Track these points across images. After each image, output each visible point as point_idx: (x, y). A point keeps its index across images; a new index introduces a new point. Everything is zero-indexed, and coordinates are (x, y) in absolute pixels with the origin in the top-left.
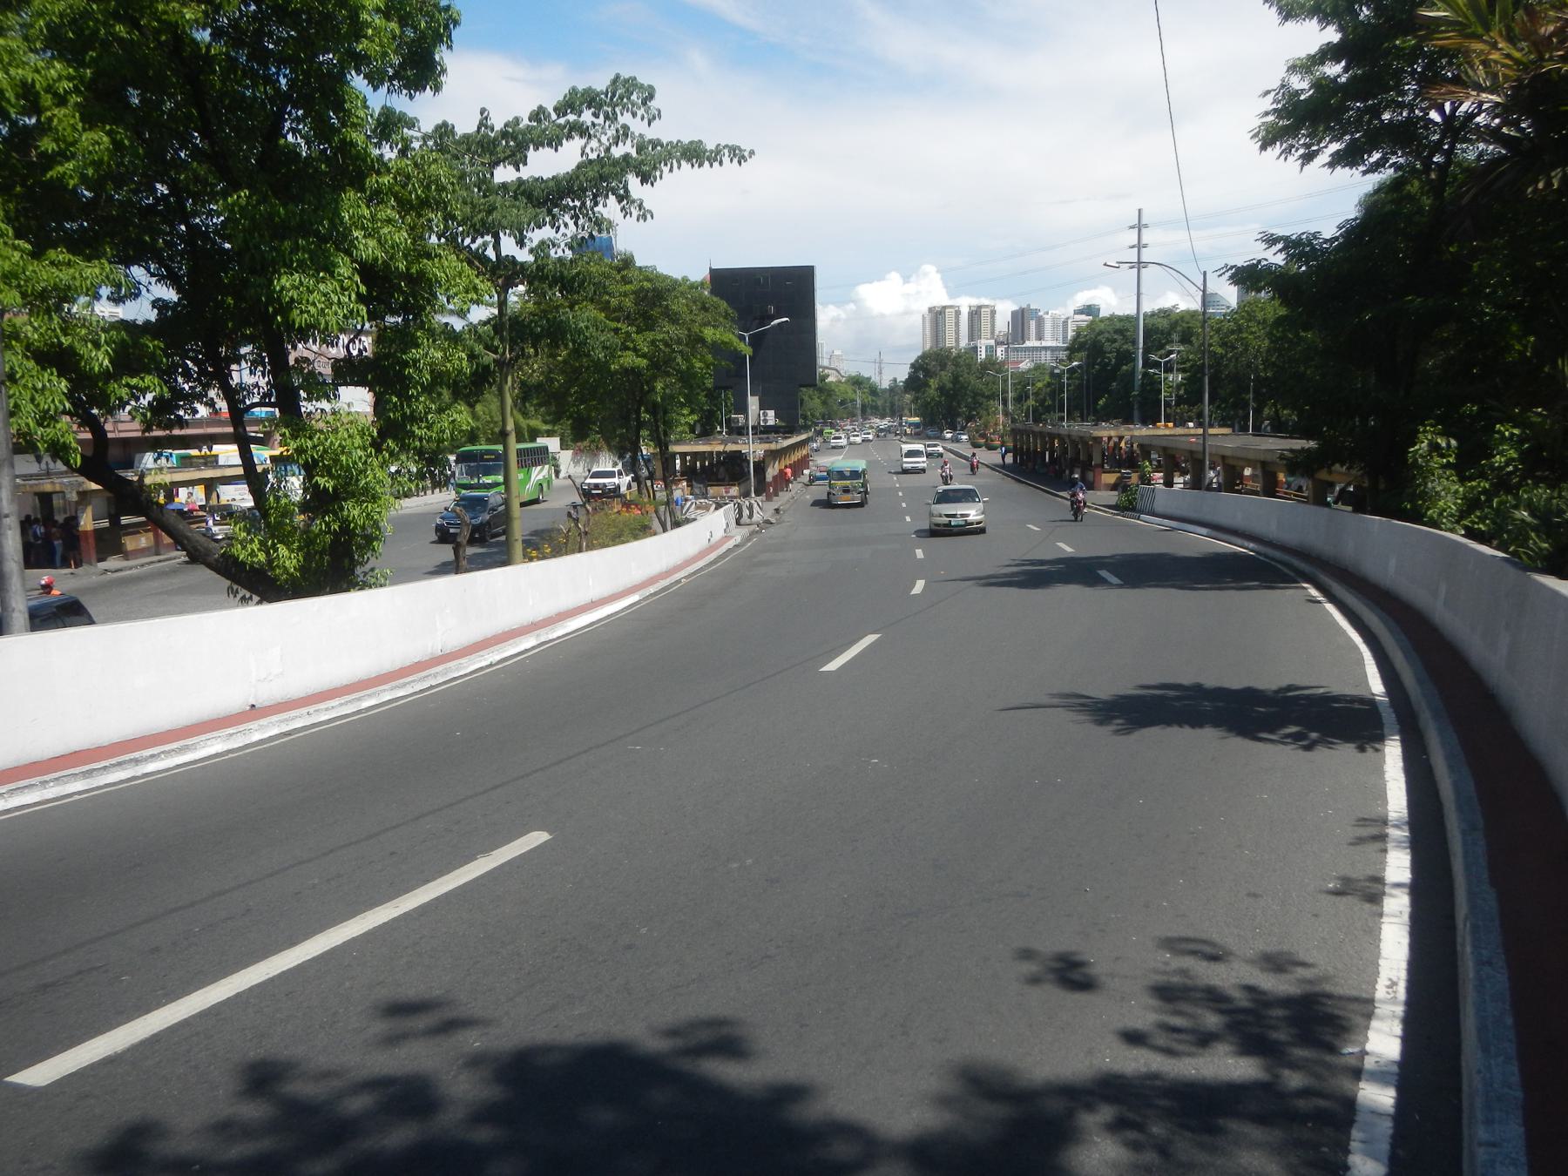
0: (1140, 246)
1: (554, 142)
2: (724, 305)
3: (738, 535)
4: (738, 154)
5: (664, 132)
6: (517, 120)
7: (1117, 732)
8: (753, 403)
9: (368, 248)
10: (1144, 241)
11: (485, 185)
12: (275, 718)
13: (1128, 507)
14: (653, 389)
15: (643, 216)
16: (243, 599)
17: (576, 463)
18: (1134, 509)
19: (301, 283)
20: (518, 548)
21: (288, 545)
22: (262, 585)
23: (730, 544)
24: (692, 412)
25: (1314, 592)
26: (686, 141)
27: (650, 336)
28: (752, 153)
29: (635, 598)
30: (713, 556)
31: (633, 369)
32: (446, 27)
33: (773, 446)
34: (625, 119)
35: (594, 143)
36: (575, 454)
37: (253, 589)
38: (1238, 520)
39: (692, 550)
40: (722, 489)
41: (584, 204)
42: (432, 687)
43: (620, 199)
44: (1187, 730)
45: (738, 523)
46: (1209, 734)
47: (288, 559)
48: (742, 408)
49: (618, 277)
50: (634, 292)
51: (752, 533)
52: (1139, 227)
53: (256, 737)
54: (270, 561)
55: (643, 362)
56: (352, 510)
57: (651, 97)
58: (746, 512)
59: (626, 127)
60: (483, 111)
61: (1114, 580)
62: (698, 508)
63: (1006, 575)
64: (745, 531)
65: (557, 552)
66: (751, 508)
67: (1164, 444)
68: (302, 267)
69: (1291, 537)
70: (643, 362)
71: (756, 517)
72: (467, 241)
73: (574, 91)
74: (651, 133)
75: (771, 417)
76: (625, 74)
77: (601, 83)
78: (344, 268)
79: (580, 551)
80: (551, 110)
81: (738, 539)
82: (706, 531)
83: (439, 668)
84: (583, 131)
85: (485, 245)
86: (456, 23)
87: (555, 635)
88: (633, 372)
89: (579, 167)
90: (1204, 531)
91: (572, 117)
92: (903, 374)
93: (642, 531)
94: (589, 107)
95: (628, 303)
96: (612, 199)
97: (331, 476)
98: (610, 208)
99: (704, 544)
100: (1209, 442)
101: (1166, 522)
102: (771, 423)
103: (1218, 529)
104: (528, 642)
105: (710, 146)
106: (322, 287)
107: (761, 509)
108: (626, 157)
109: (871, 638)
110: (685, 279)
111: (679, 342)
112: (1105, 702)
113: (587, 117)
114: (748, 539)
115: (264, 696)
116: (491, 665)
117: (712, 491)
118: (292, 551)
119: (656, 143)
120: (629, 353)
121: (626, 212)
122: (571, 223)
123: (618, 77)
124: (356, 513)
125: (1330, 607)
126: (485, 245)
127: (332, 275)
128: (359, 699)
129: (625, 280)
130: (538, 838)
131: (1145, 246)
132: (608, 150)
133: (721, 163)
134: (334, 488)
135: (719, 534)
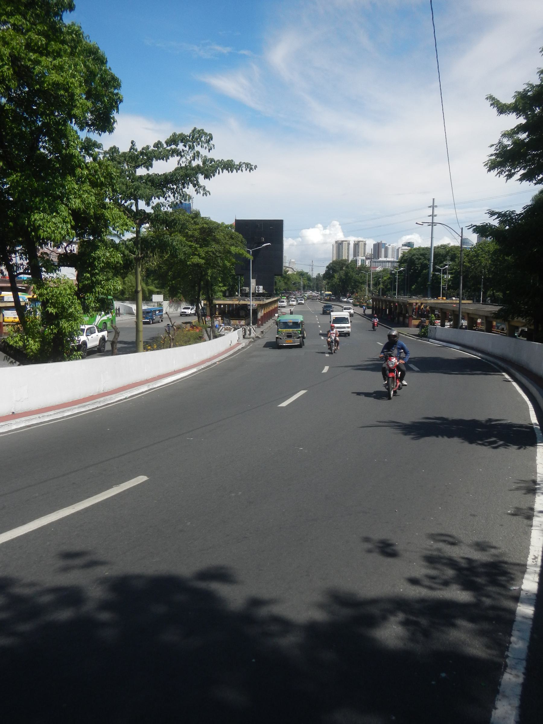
0: (433, 216)
1: (164, 156)
2: (241, 235)
3: (244, 343)
4: (250, 167)
5: (217, 154)
6: (148, 147)
7: (413, 439)
8: (253, 282)
9: (76, 203)
10: (435, 214)
11: (132, 175)
12: (23, 419)
13: (424, 335)
14: (206, 274)
15: (205, 194)
16: (11, 362)
17: (170, 307)
18: (426, 337)
19: (44, 218)
20: (141, 345)
21: (34, 338)
22: (20, 356)
23: (240, 347)
24: (224, 286)
25: (507, 377)
26: (226, 160)
27: (206, 249)
28: (256, 167)
29: (194, 370)
30: (231, 352)
31: (198, 264)
32: (116, 103)
33: (261, 303)
34: (198, 148)
35: (184, 159)
36: (170, 303)
37: (17, 360)
38: (473, 343)
39: (222, 349)
40: (237, 322)
41: (178, 187)
42: (98, 407)
43: (194, 186)
44: (446, 438)
45: (244, 337)
46: (456, 441)
47: (34, 345)
48: (248, 285)
49: (192, 222)
50: (199, 229)
51: (250, 342)
52: (433, 207)
53: (14, 427)
54: (25, 346)
55: (203, 261)
56: (64, 324)
57: (211, 138)
58: (248, 332)
59: (198, 153)
60: (132, 142)
61: (416, 369)
62: (226, 330)
63: (365, 365)
64: (247, 341)
65: (159, 347)
66: (250, 331)
67: (441, 307)
68: (44, 211)
69: (497, 351)
70: (203, 261)
71: (253, 335)
72: (123, 202)
73: (174, 135)
74: (210, 156)
75: (261, 289)
76: (199, 128)
77: (187, 131)
78: (64, 211)
79: (170, 347)
80: (163, 143)
81: (243, 345)
82: (229, 340)
83: (102, 399)
84: (178, 153)
85: (132, 204)
86: (121, 101)
87: (156, 386)
88: (198, 265)
89: (176, 170)
90: (458, 347)
91: (173, 147)
93: (199, 339)
94: (182, 142)
95: (196, 234)
96: (191, 185)
97: (55, 307)
98: (190, 190)
99: (228, 346)
100: (461, 307)
102: (261, 291)
103: (465, 347)
104: (144, 388)
105: (237, 163)
106: (54, 220)
107: (254, 331)
108: (198, 166)
109: (302, 392)
110: (223, 223)
111: (220, 252)
112: (409, 425)
113: (181, 146)
114: (248, 345)
115: (19, 408)
116: (126, 398)
117: (232, 322)
118: (35, 342)
119: (212, 160)
120: (197, 257)
121: (197, 192)
122: (172, 196)
123: (195, 129)
124: (66, 325)
125: (514, 384)
126: (132, 204)
127: (58, 213)
128: (63, 412)
129: (196, 223)
130: (142, 479)
131: (436, 216)
132: (190, 162)
133: (242, 170)
134: (56, 313)
135: (235, 342)
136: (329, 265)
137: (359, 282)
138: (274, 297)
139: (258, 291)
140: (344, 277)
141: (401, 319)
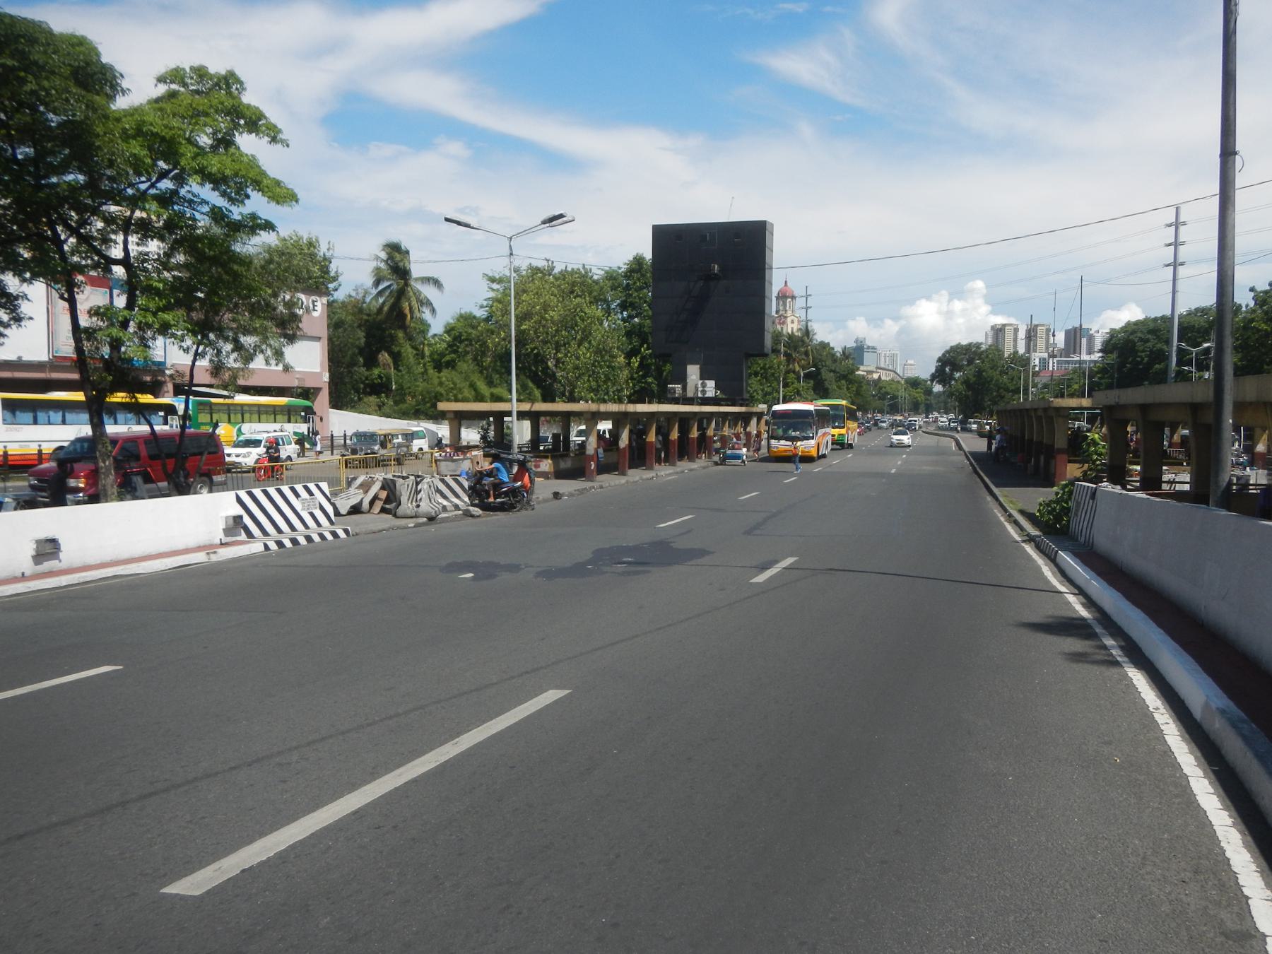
0: (1176, 244)
8: (693, 371)
10: (1181, 239)
48: (682, 379)
52: (1177, 224)
75: (711, 388)
92: (924, 368)
101: (1096, 586)
131: (1183, 244)
136: (944, 355)
137: (1007, 390)
138: (741, 405)
139: (704, 392)
140: (973, 380)
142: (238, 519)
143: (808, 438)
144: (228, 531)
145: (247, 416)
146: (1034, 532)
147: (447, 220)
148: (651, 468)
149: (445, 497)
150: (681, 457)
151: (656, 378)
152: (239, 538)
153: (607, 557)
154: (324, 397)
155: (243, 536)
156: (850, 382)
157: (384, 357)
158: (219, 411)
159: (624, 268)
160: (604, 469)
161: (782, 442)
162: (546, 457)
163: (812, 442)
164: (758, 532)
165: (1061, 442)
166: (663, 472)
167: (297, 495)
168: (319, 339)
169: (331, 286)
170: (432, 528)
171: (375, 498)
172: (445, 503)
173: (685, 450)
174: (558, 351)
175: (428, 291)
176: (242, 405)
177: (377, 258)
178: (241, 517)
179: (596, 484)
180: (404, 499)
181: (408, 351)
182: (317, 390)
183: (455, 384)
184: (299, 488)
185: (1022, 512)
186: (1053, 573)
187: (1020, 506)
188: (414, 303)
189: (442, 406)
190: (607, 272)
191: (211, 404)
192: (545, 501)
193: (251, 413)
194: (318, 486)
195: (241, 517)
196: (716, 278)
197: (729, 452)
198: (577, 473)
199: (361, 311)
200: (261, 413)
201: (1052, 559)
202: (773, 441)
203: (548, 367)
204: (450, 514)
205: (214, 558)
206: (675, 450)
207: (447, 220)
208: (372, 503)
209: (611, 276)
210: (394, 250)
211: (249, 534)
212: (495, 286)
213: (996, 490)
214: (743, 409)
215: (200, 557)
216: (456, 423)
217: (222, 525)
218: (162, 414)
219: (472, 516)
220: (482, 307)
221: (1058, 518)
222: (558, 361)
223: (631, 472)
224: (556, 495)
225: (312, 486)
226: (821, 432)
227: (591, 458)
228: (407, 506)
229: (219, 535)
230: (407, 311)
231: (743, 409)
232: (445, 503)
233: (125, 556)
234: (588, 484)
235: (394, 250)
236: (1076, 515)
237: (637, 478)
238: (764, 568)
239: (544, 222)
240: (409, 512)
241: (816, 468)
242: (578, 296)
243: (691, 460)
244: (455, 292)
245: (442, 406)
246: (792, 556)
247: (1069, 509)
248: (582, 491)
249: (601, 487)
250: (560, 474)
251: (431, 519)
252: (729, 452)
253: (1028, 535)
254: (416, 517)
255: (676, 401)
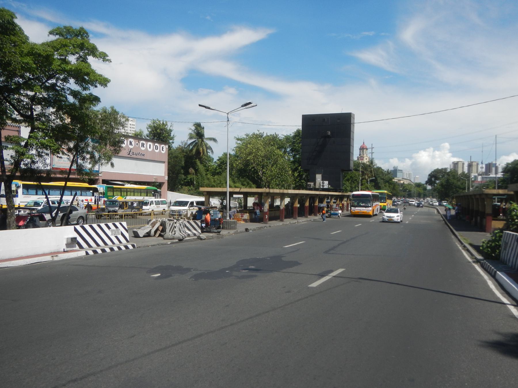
8: (319, 177)
48: (314, 180)
75: (326, 184)
92: (422, 179)
136: (431, 173)
137: (460, 188)
138: (340, 192)
139: (323, 186)
140: (445, 183)
141: (479, 218)
142: (74, 240)
143: (368, 207)
144: (68, 245)
145: (129, 193)
146: (480, 257)
147: (200, 105)
148: (295, 218)
149: (189, 230)
150: (310, 214)
151: (304, 179)
152: (74, 249)
153: (243, 265)
154: (165, 186)
155: (77, 247)
156: (390, 184)
157: (192, 170)
158: (117, 191)
159: (292, 135)
160: (271, 219)
161: (357, 208)
162: (246, 213)
163: (370, 208)
164: (332, 252)
165: (489, 210)
166: (302, 221)
167: (109, 228)
168: (164, 162)
169: (171, 141)
170: (181, 243)
171: (157, 230)
172: (189, 233)
173: (313, 210)
174: (263, 168)
175: (210, 143)
176: (127, 189)
177: (191, 129)
178: (76, 238)
179: (267, 225)
180: (168, 230)
181: (201, 167)
182: (163, 183)
183: (220, 181)
184: (110, 224)
185: (471, 245)
186: (496, 286)
187: (469, 241)
188: (205, 148)
189: (202, 189)
190: (285, 136)
191: (113, 188)
192: (241, 232)
193: (130, 192)
194: (121, 224)
195: (76, 238)
196: (328, 137)
197: (332, 212)
198: (260, 220)
199: (183, 151)
200: (134, 191)
201: (493, 276)
202: (352, 208)
203: (259, 175)
204: (191, 238)
205: (56, 259)
206: (307, 210)
207: (200, 105)
208: (156, 232)
209: (287, 138)
210: (198, 126)
211: (81, 247)
212: (239, 142)
213: (457, 233)
214: (340, 194)
215: (48, 258)
216: (208, 197)
217: (65, 242)
218: (91, 191)
219: (201, 239)
220: (233, 150)
221: (493, 251)
222: (263, 173)
223: (285, 220)
224: (247, 230)
225: (117, 224)
226: (375, 204)
227: (266, 213)
228: (168, 233)
229: (63, 247)
230: (201, 151)
231: (340, 194)
232: (189, 233)
233: (7, 257)
234: (265, 225)
235: (198, 126)
236: (505, 249)
237: (288, 223)
238: (322, 275)
239: (242, 106)
240: (169, 237)
241: (372, 220)
242: (272, 145)
243: (316, 215)
244: (222, 145)
245: (202, 189)
246: (342, 268)
247: (500, 246)
248: (260, 228)
249: (270, 226)
250: (252, 220)
251: (180, 240)
252: (332, 212)
253: (476, 258)
254: (173, 239)
255: (311, 189)
